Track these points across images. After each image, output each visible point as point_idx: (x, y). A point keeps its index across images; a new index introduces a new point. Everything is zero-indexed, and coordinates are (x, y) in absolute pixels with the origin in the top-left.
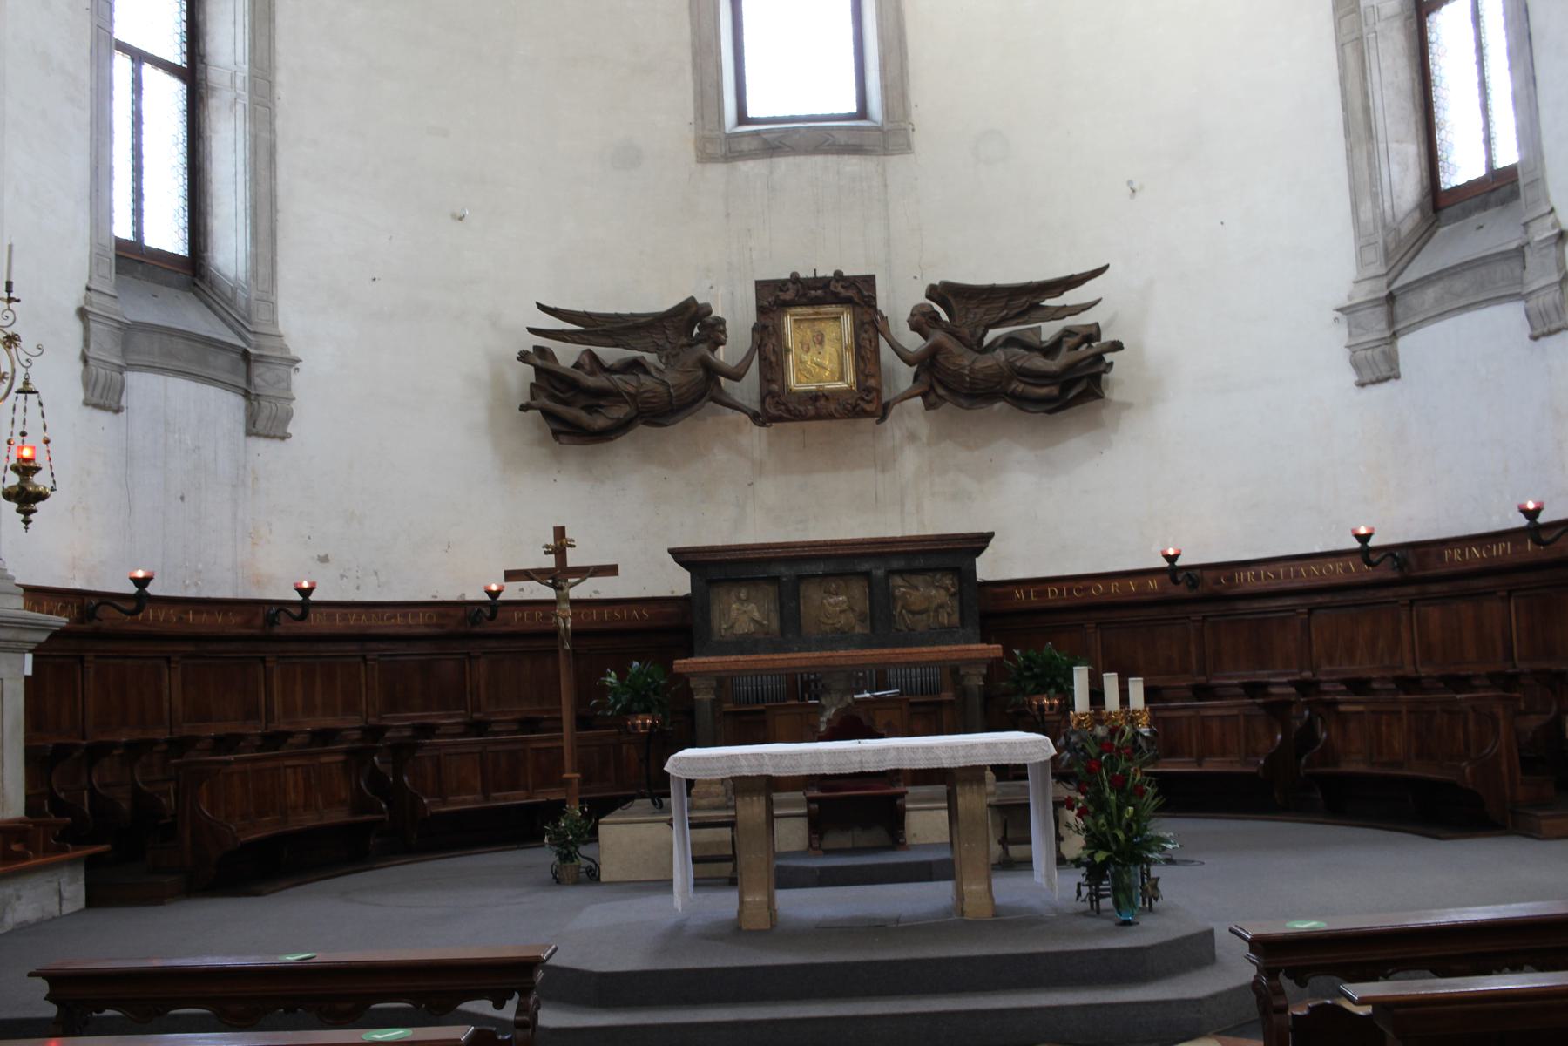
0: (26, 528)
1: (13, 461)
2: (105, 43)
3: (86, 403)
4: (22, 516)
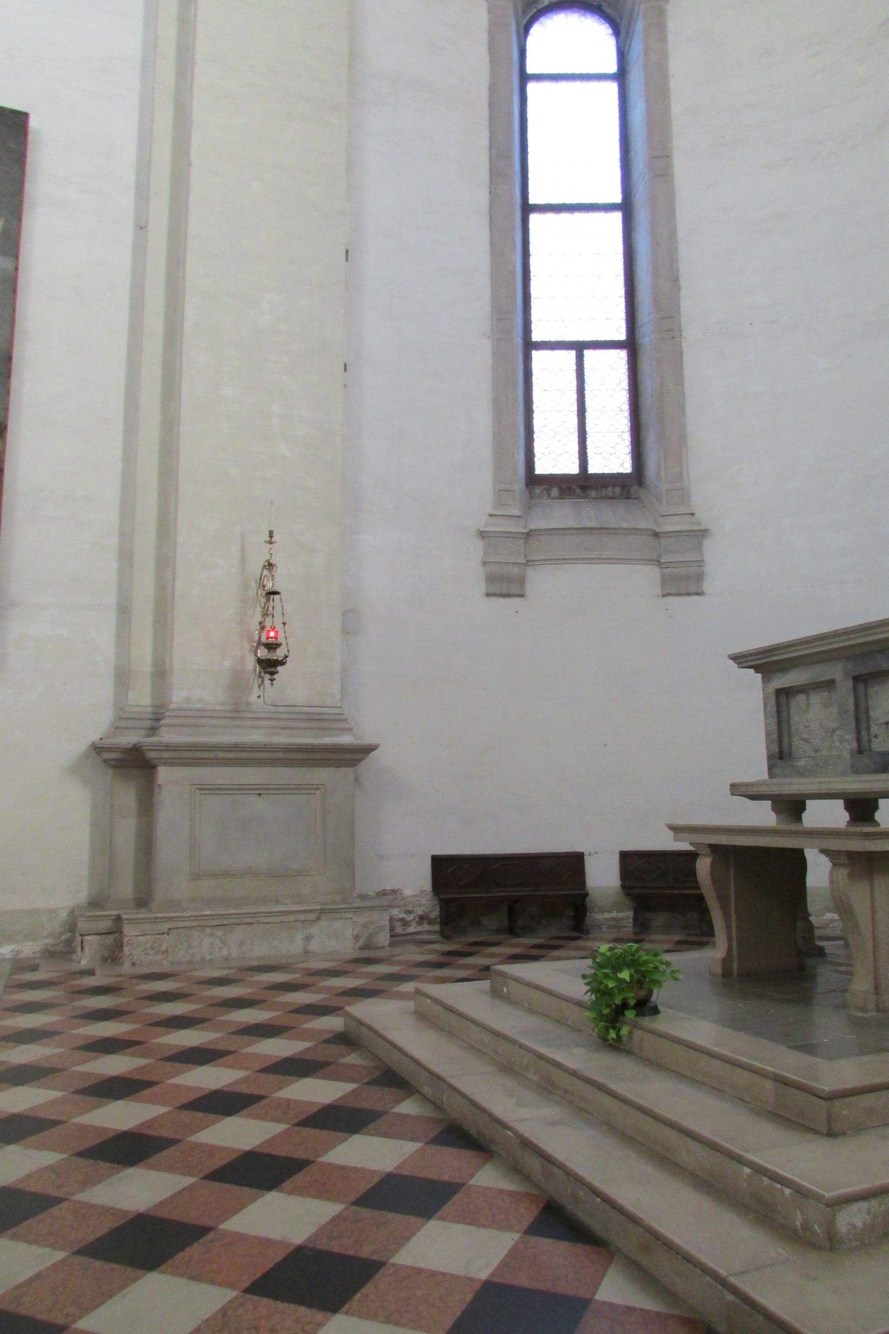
0: (272, 684)
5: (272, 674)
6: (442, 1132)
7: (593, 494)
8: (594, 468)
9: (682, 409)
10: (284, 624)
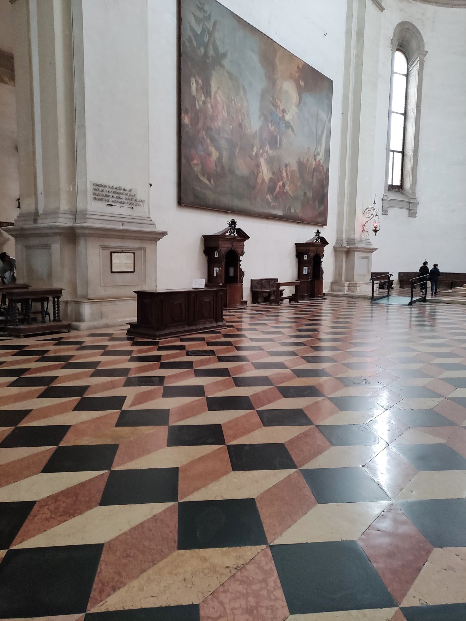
1: (374, 226)
2: (388, 150)
3: (382, 214)
4: (375, 234)
5: (376, 233)
6: (417, 316)
7: (393, 190)
8: (394, 184)
9: (416, 173)
10: (379, 223)
